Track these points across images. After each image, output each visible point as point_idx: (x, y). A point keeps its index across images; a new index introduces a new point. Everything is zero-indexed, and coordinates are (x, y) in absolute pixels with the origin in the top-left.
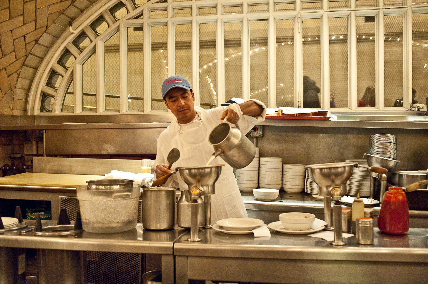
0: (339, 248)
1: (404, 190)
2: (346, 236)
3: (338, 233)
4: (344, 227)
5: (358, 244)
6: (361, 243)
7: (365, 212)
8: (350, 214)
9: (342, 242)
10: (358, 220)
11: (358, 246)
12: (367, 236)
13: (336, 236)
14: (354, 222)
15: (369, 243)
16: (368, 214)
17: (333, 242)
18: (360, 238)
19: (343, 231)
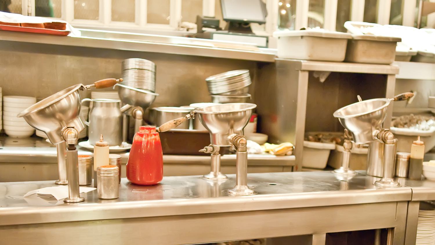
0: (75, 206)
1: (157, 131)
2: (84, 190)
3: (75, 186)
4: (82, 178)
5: (100, 199)
6: (103, 198)
7: (110, 159)
8: (91, 162)
9: (78, 198)
10: (99, 169)
11: (100, 202)
12: (110, 188)
13: (70, 191)
14: (95, 172)
15: (113, 197)
16: (113, 162)
17: (67, 198)
18: (103, 191)
19: (80, 184)
